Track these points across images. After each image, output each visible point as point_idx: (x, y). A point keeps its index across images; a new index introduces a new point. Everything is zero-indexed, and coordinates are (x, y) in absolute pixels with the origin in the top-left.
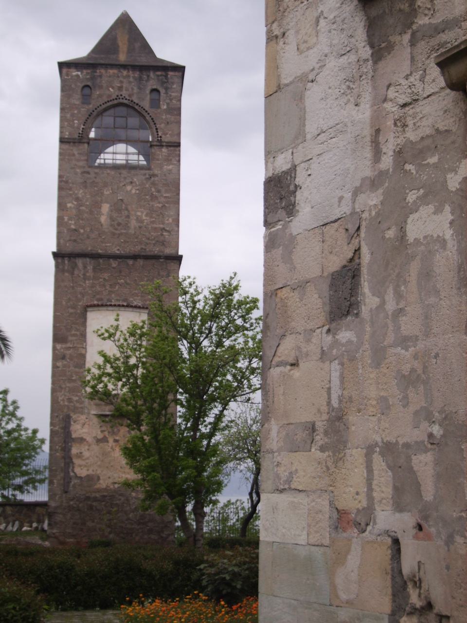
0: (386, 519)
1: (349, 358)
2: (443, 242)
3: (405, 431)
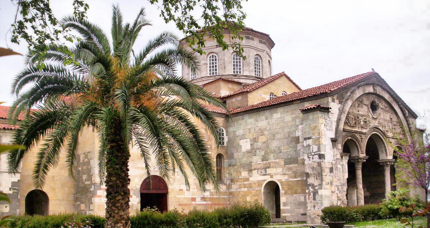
1: (332, 176)
3: (338, 184)
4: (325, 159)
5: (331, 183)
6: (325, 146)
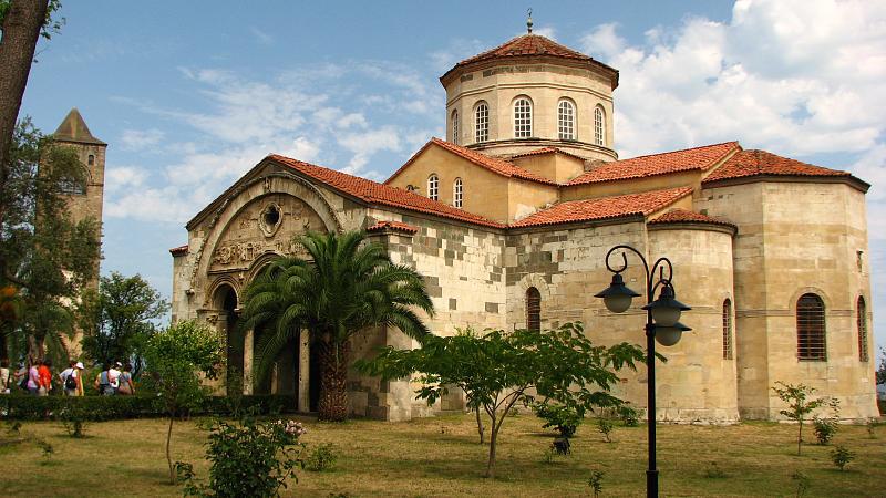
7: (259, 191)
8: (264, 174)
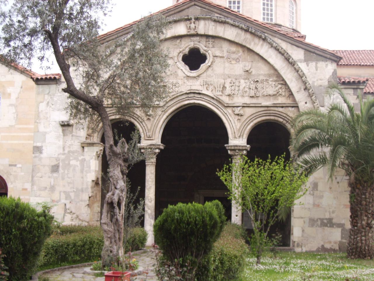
0: (63, 201)
2: (78, 166)
3: (68, 189)
4: (41, 153)
5: (52, 189)
6: (44, 134)
7: (181, 29)
8: (183, 15)
